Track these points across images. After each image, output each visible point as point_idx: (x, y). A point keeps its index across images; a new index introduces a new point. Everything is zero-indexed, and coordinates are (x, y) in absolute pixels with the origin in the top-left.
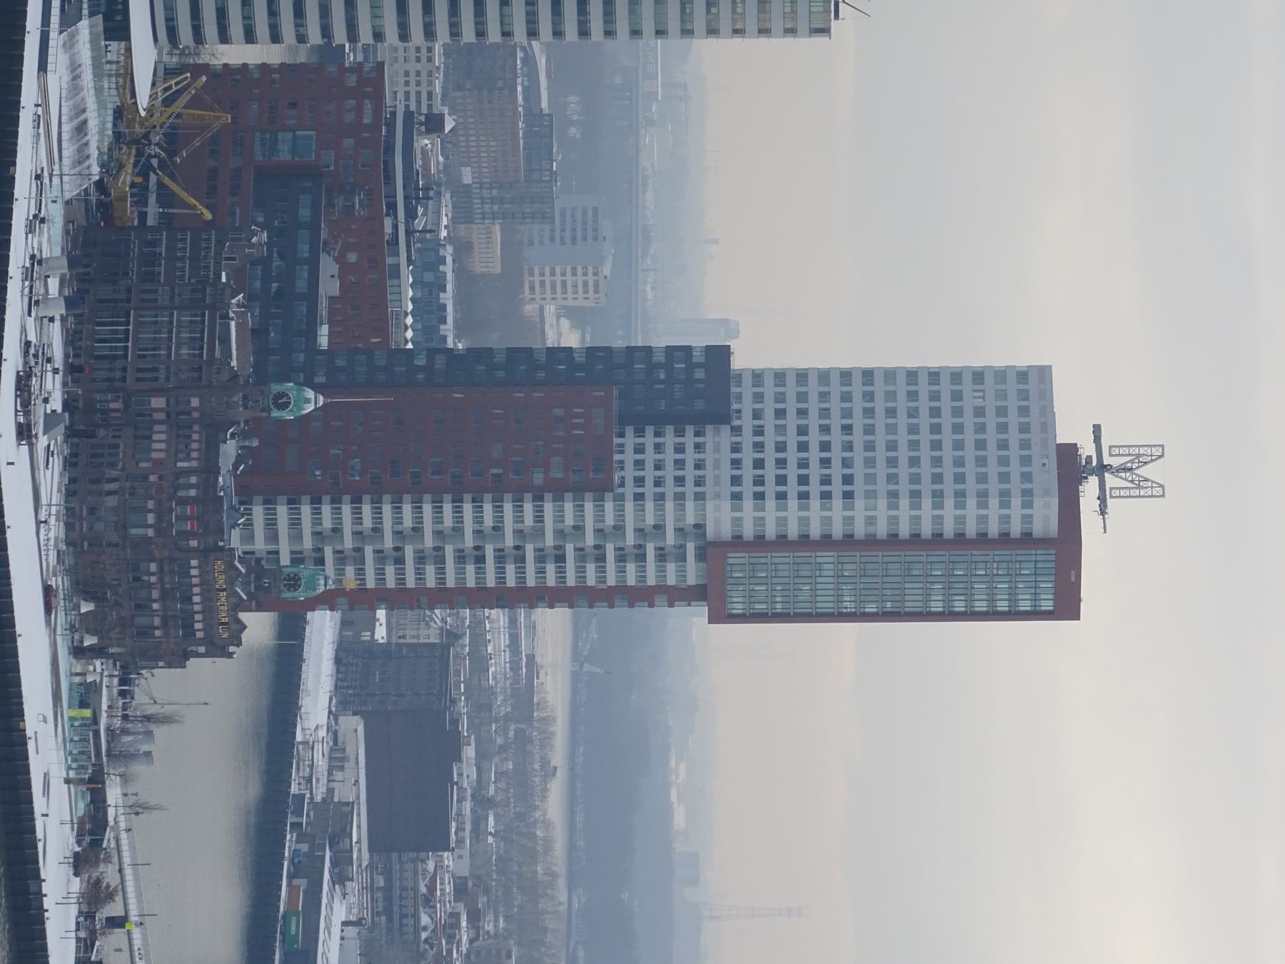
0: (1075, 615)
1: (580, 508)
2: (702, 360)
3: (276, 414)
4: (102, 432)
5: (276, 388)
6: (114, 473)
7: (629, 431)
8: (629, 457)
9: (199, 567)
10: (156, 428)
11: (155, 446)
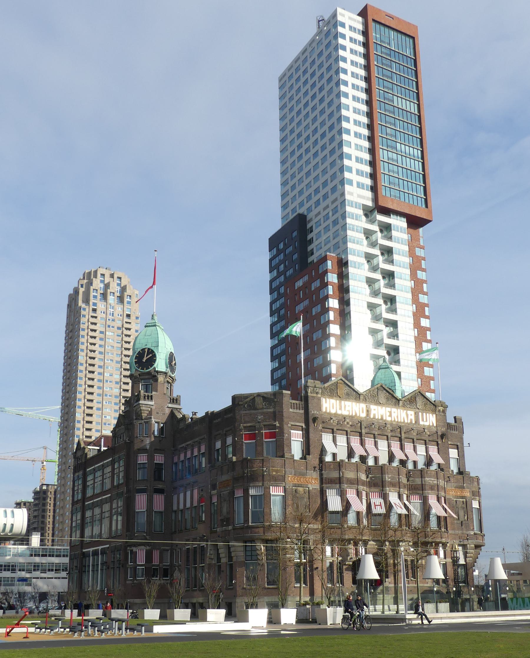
10: (175, 508)
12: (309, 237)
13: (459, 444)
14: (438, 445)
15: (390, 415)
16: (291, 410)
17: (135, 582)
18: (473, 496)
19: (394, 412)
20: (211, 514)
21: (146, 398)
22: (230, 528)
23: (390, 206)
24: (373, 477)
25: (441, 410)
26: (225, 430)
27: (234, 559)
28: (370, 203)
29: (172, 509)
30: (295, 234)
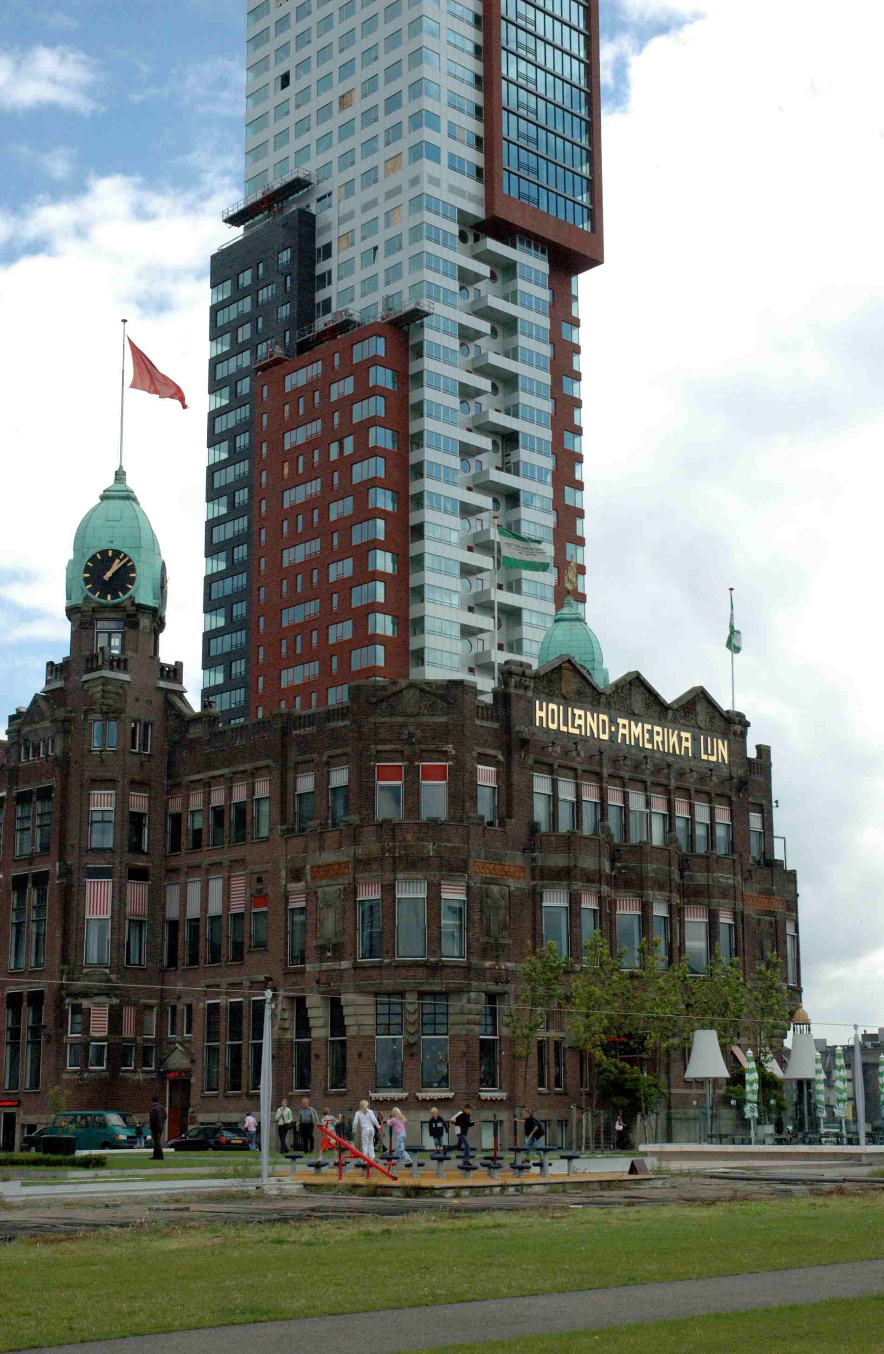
4: (177, 1060)
12: (321, 268)
13: (764, 802)
14: (730, 803)
15: (651, 740)
16: (478, 722)
17: (86, 1075)
18: (788, 910)
19: (658, 733)
20: (287, 932)
21: (115, 663)
22: (345, 964)
23: (516, 218)
24: (621, 868)
25: (739, 731)
26: (327, 753)
27: (351, 1031)
28: (477, 211)
29: (164, 915)
30: (285, 256)
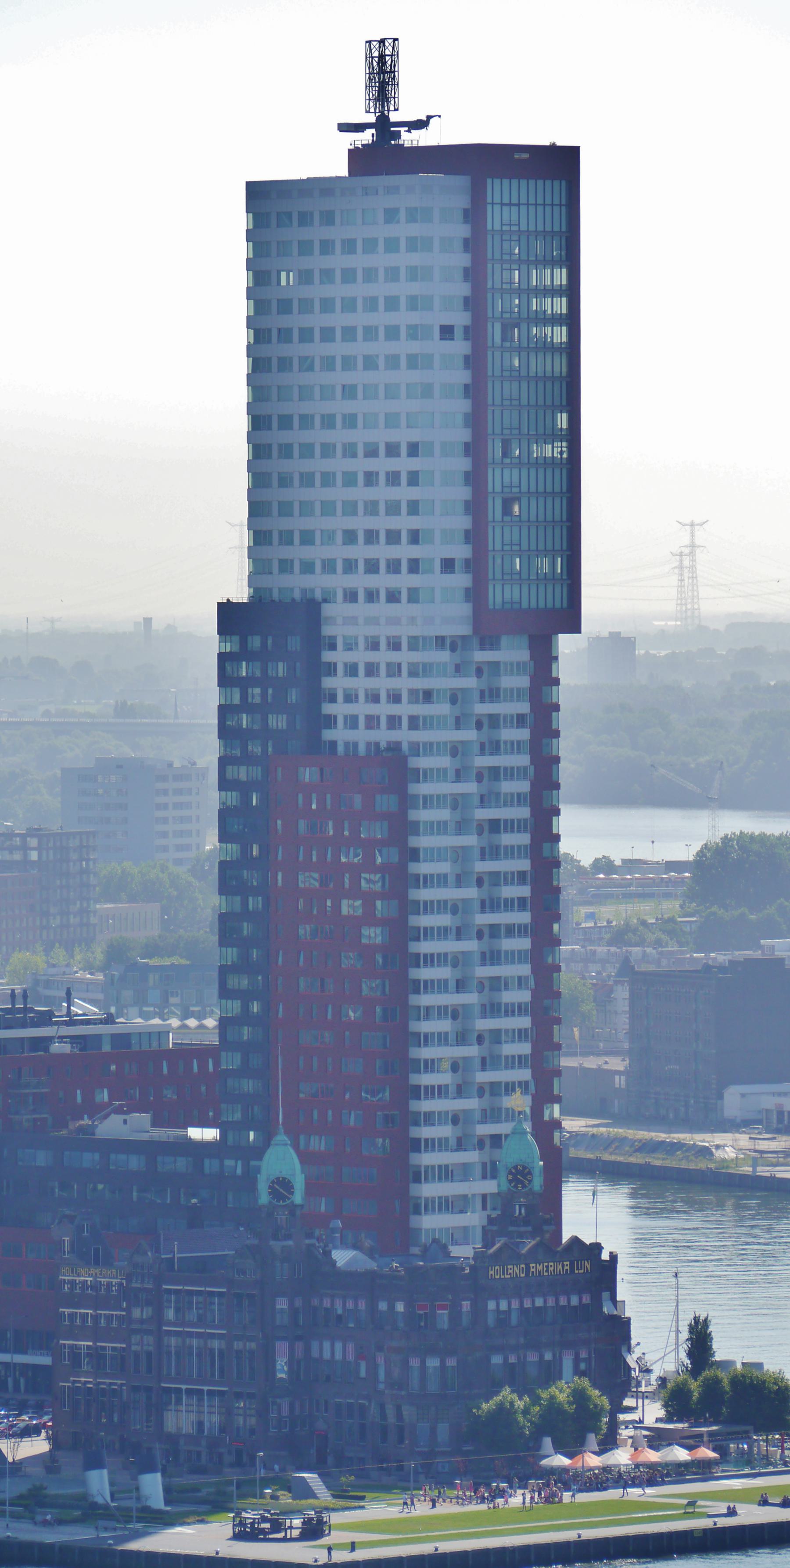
0: (574, 152)
1: (428, 801)
2: (236, 638)
3: (298, 1197)
5: (264, 1198)
6: (373, 1410)
7: (328, 735)
8: (362, 736)
9: (497, 1298)
10: (315, 1354)
11: (339, 1356)
15: (547, 1271)
22: (403, 1393)
